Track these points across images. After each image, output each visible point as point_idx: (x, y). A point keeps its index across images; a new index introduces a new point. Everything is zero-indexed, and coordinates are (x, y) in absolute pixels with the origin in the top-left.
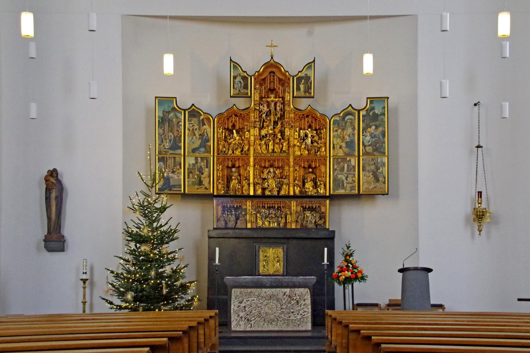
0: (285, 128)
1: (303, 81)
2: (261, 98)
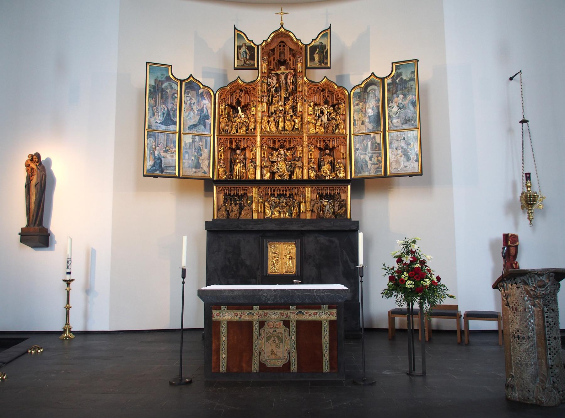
0: (297, 104)
1: (318, 50)
2: (270, 70)
